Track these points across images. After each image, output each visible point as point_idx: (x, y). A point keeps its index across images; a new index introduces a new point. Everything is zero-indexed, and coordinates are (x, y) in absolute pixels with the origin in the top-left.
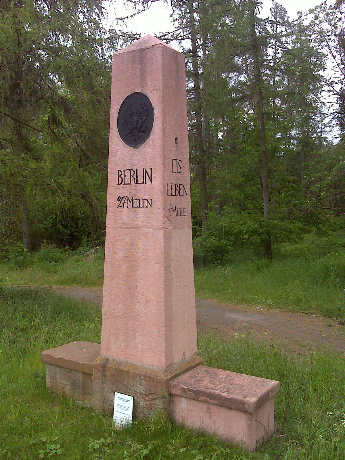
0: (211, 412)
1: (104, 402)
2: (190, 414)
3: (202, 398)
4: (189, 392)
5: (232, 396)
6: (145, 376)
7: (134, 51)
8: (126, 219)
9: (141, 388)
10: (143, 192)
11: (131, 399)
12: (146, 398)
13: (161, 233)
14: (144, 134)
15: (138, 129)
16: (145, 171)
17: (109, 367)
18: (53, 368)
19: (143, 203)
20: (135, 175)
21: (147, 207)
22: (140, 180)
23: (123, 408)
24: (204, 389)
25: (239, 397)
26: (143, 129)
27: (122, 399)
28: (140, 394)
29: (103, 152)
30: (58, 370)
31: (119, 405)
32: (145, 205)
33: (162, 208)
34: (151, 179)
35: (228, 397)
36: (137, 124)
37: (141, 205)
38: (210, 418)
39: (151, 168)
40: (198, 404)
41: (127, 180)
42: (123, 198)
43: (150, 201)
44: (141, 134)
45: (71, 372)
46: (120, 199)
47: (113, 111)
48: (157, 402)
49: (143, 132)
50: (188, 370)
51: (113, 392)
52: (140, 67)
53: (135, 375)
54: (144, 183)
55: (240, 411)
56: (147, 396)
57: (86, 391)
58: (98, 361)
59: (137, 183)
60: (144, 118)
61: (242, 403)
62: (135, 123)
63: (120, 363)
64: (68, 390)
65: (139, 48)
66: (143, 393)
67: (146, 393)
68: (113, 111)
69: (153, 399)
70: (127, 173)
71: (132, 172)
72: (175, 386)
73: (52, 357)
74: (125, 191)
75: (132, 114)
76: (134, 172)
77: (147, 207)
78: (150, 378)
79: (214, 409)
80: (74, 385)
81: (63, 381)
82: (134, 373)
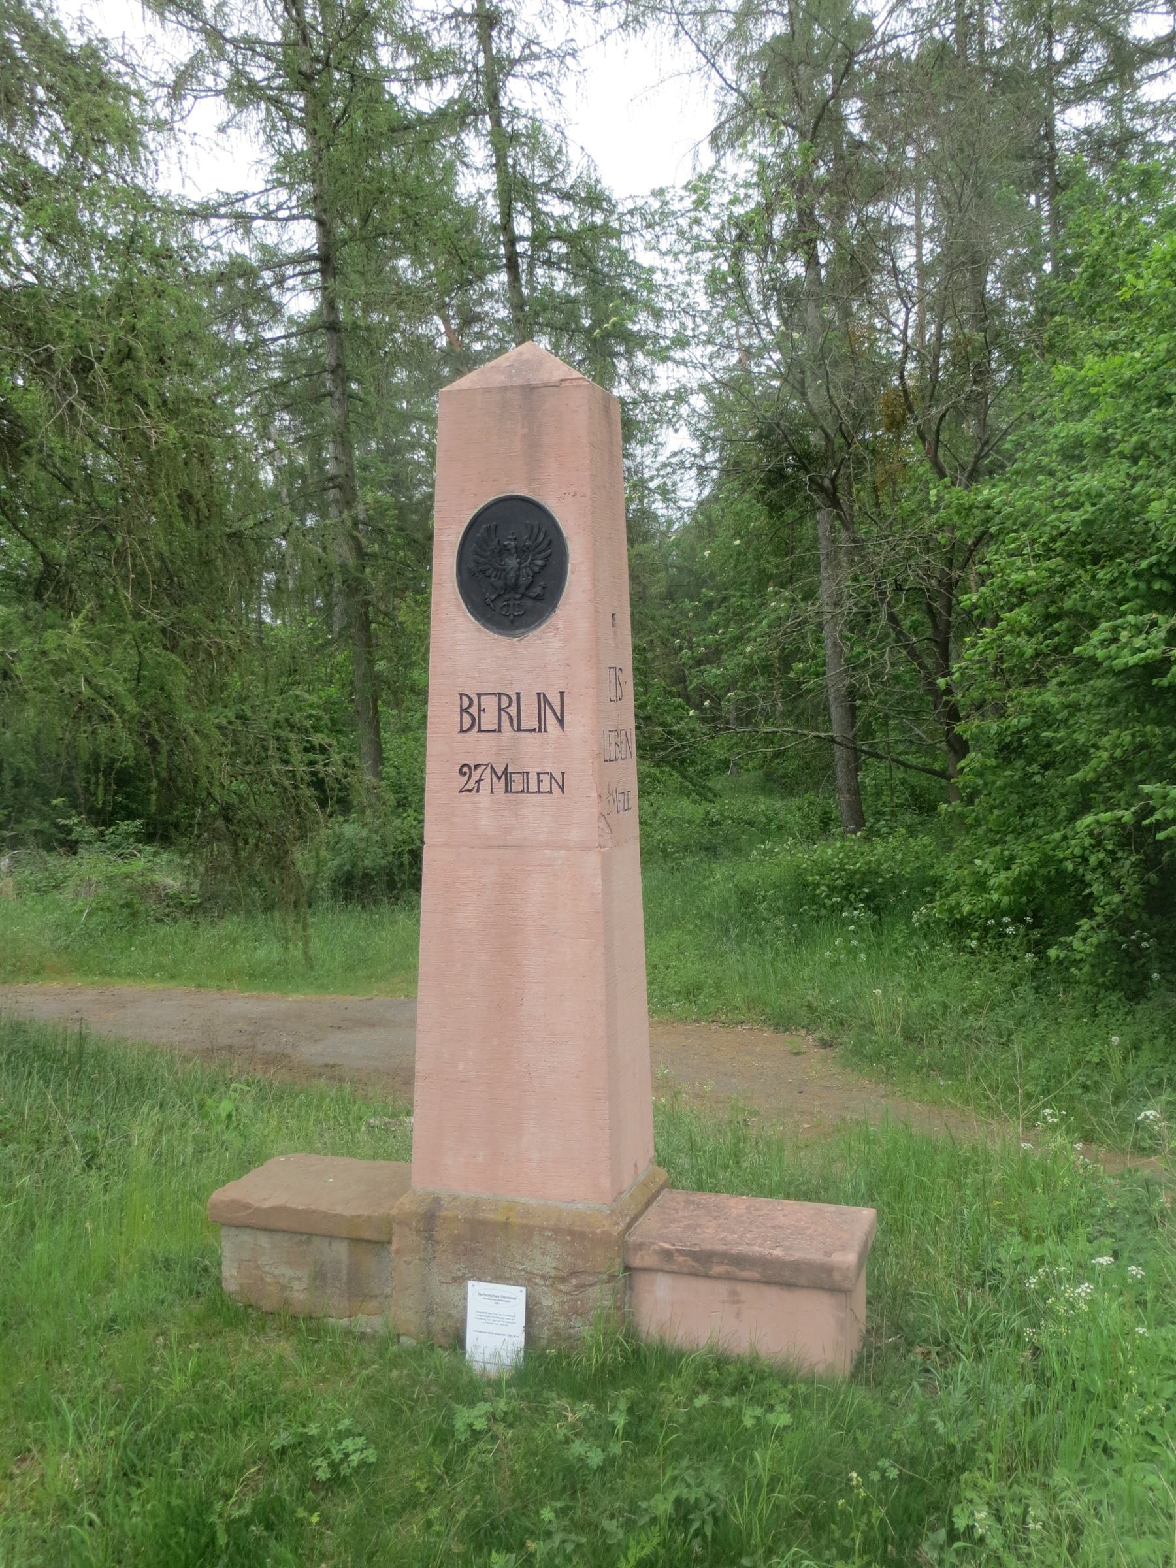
0: (738, 1302)
1: (430, 1312)
2: (676, 1313)
3: (717, 1269)
4: (681, 1259)
5: (797, 1255)
6: (557, 1231)
7: (503, 389)
9: (548, 1262)
10: (535, 753)
12: (562, 1287)
13: (593, 860)
14: (538, 604)
15: (522, 590)
17: (445, 1218)
18: (246, 1237)
19: (539, 781)
20: (513, 710)
21: (551, 792)
22: (530, 721)
23: (495, 1323)
24: (720, 1247)
25: (815, 1256)
26: (537, 590)
27: (489, 1297)
28: (543, 1277)
29: (412, 648)
30: (264, 1240)
31: (481, 1315)
32: (545, 787)
33: (594, 795)
34: (561, 722)
35: (787, 1258)
36: (518, 577)
37: (533, 786)
38: (738, 1315)
39: (562, 693)
40: (702, 1285)
41: (489, 720)
42: (476, 767)
43: (559, 777)
44: (528, 603)
45: (308, 1242)
46: (465, 769)
47: (444, 538)
48: (595, 1292)
49: (538, 598)
50: (648, 1204)
51: (460, 1280)
52: (525, 430)
53: (527, 1232)
54: (541, 729)
55: (822, 1289)
56: (563, 1280)
57: (357, 1289)
58: (406, 1204)
59: (519, 730)
60: (540, 563)
61: (828, 1270)
62: (512, 574)
63: (477, 1204)
64: (299, 1294)
65: (518, 381)
66: (553, 1273)
67: (559, 1273)
68: (444, 538)
69: (581, 1287)
70: (490, 704)
71: (505, 702)
72: (640, 1246)
73: (246, 1207)
74: (481, 748)
75: (503, 551)
76: (509, 703)
77: (551, 792)
78: (574, 1235)
79: (748, 1292)
80: (320, 1277)
81: (287, 1272)
82: (524, 1226)
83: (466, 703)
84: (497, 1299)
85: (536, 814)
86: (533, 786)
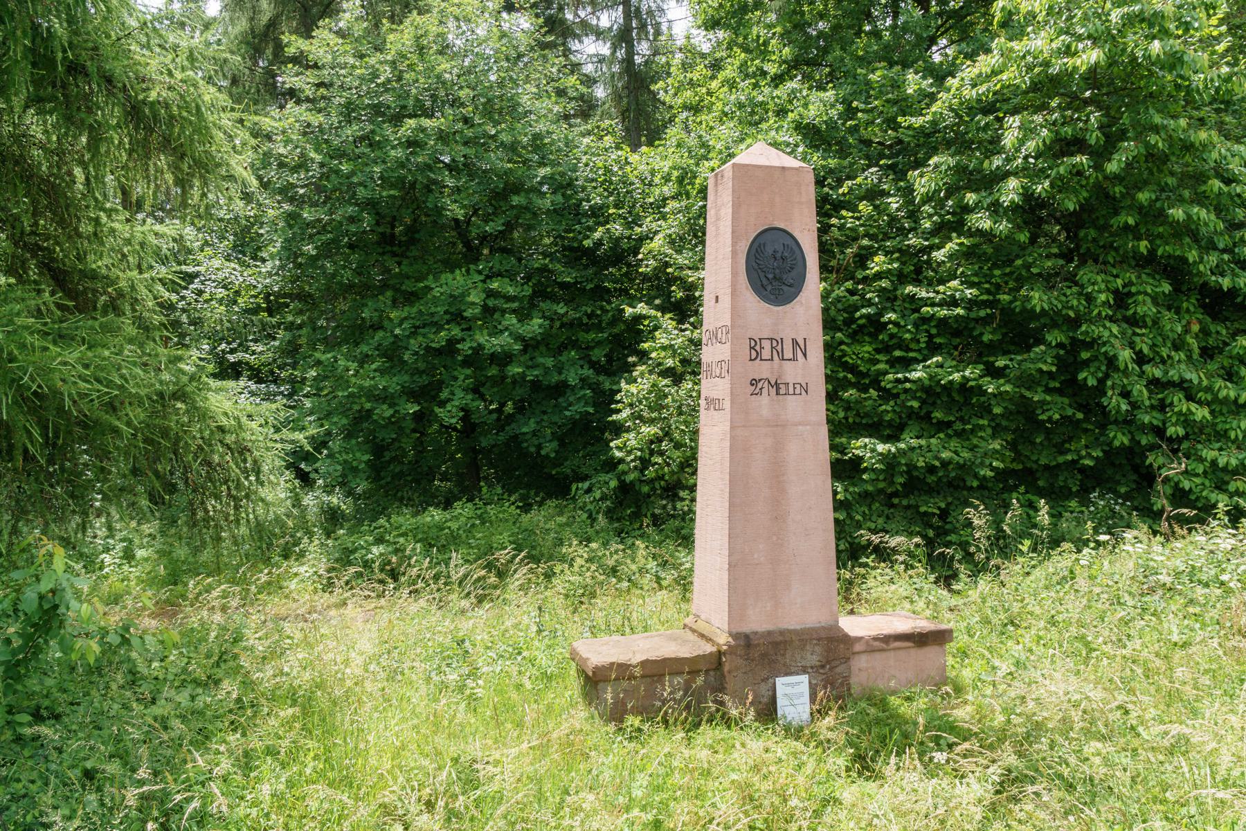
8: (765, 412)
10: (792, 372)
11: (804, 679)
16: (795, 342)
20: (779, 348)
32: (798, 391)
34: (805, 355)
37: (791, 391)
41: (766, 354)
54: (794, 359)
56: (823, 667)
63: (769, 633)
69: (831, 669)
70: (766, 344)
71: (775, 344)
74: (763, 370)
83: (753, 343)
84: (792, 685)
85: (793, 406)
86: (791, 391)
